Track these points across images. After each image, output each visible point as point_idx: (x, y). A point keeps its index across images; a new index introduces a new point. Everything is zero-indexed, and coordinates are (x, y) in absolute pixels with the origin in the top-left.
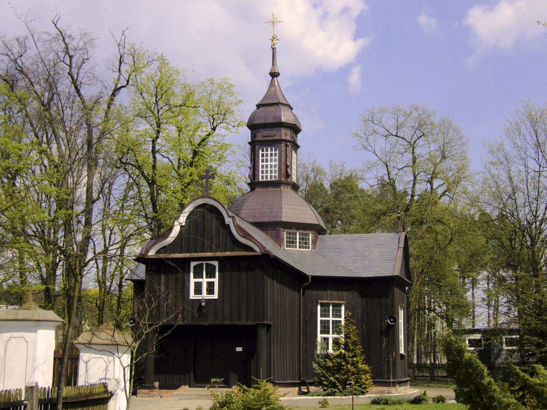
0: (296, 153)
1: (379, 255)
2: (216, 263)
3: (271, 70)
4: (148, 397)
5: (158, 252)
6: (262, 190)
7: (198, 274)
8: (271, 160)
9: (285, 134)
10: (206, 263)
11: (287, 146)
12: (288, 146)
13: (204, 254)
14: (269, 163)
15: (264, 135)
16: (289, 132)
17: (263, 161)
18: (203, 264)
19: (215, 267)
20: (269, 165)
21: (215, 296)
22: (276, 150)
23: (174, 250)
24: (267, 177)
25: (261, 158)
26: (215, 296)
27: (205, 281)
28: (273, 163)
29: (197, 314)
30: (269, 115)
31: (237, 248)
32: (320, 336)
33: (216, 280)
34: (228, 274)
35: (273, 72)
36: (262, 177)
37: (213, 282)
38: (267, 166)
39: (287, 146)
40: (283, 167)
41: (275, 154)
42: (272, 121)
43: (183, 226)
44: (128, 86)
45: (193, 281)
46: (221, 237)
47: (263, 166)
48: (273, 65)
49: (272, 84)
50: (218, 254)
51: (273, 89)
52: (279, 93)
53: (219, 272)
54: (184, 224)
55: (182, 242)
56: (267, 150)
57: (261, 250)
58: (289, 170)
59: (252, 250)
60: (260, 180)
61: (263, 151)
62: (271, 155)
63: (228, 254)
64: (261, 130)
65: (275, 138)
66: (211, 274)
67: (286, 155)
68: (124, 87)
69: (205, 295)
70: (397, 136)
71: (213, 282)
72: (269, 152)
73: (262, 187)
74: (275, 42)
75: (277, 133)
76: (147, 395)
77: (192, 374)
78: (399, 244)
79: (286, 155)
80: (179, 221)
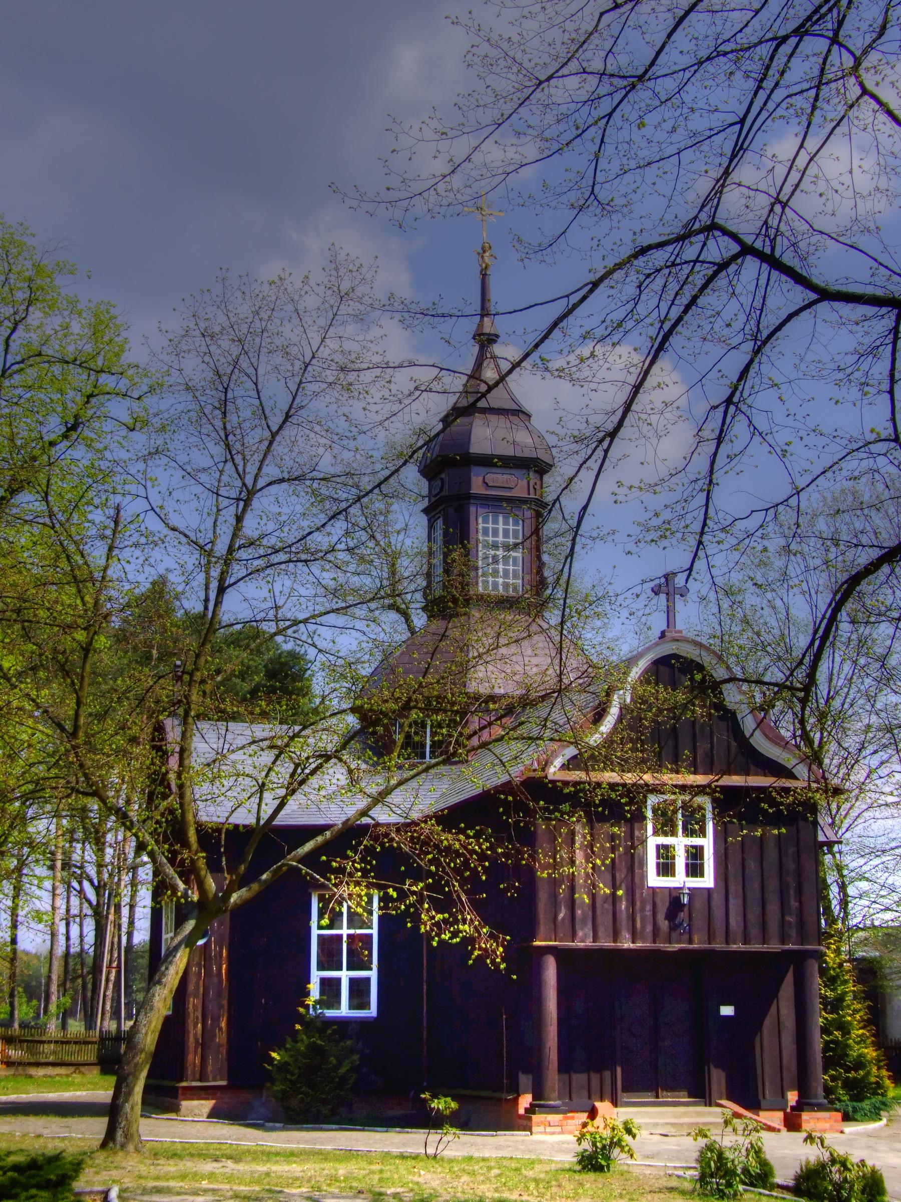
2: (704, 801)
4: (562, 1133)
7: (666, 826)
21: (707, 881)
22: (516, 523)
26: (707, 881)
27: (680, 843)
29: (664, 924)
31: (752, 767)
32: (316, 975)
33: (707, 843)
37: (701, 848)
45: (653, 842)
56: (495, 522)
61: (486, 521)
63: (736, 780)
64: (482, 470)
66: (694, 827)
69: (680, 879)
71: (701, 848)
72: (501, 526)
76: (559, 1129)
77: (619, 1070)
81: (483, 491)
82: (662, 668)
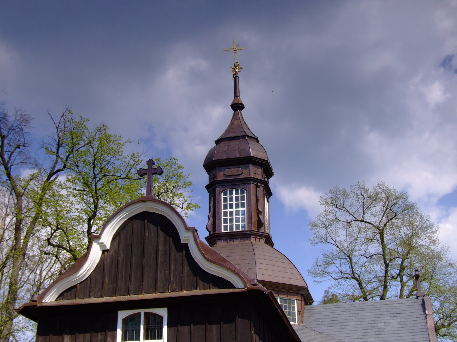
0: (268, 202)
1: (399, 326)
2: (163, 312)
3: (234, 100)
5: (61, 296)
6: (225, 243)
8: (237, 206)
9: (255, 172)
10: (146, 314)
11: (257, 187)
12: (259, 187)
13: (141, 295)
14: (234, 210)
15: (227, 174)
16: (259, 171)
17: (225, 207)
18: (139, 314)
19: (161, 318)
20: (234, 213)
22: (243, 192)
23: (90, 292)
24: (231, 227)
25: (223, 203)
28: (240, 209)
30: (234, 150)
31: (201, 283)
34: (185, 329)
35: (236, 102)
36: (226, 228)
38: (231, 213)
39: (257, 187)
40: (254, 214)
41: (243, 198)
42: (237, 155)
43: (107, 251)
44: (65, 170)
46: (173, 267)
47: (225, 214)
48: (236, 95)
49: (235, 117)
50: (168, 294)
51: (236, 122)
52: (244, 126)
53: (169, 326)
54: (108, 247)
55: (103, 277)
56: (231, 193)
57: (245, 283)
58: (261, 217)
59: (229, 285)
60: (223, 231)
61: (225, 194)
62: (237, 199)
63: (184, 293)
65: (241, 177)
67: (257, 199)
68: (62, 170)
70: (363, 221)
72: (234, 196)
73: (225, 240)
74: (237, 70)
75: (244, 171)
78: (424, 312)
79: (257, 199)
80: (101, 241)
81: (224, 178)
82: (136, 222)
